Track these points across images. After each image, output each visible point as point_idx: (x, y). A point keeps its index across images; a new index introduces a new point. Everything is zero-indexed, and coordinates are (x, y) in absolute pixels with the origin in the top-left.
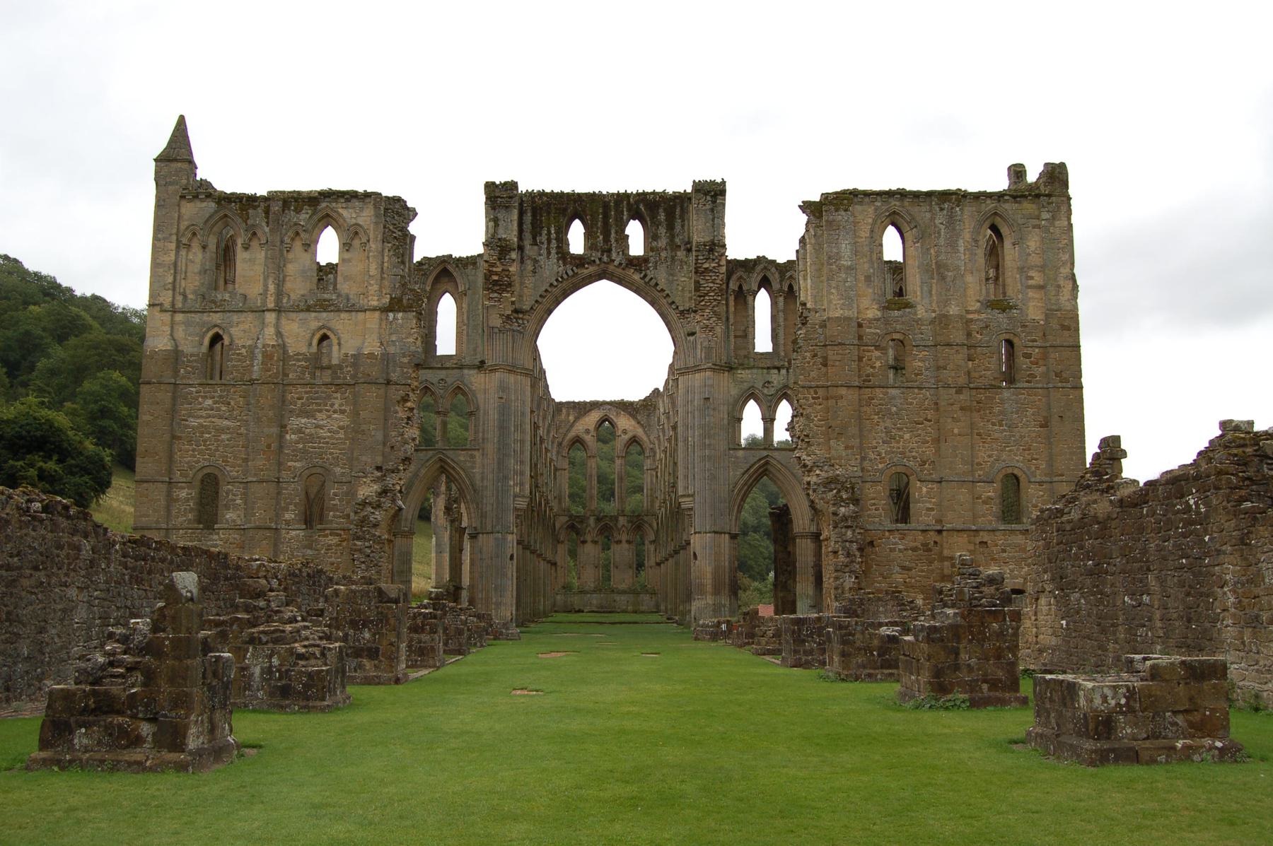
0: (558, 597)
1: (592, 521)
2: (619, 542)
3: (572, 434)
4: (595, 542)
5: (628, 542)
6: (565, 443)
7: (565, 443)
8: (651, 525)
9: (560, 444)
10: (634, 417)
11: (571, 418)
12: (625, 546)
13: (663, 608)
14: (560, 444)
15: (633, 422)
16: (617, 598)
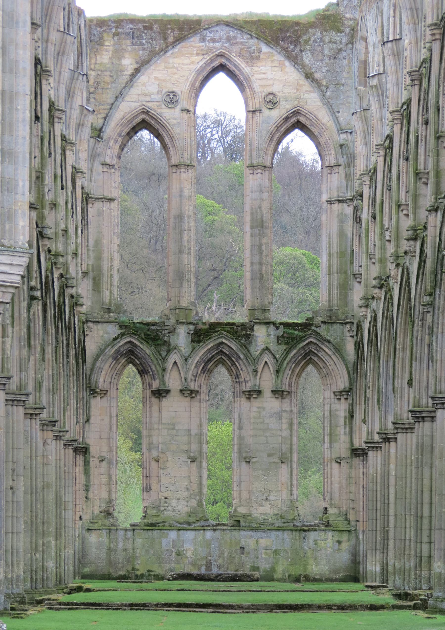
0: (93, 538)
1: (182, 338)
2: (254, 393)
3: (128, 107)
4: (189, 393)
5: (277, 393)
6: (112, 130)
7: (112, 130)
8: (339, 350)
9: (98, 133)
10: (295, 60)
11: (128, 63)
12: (270, 403)
13: (373, 566)
14: (98, 133)
15: (292, 74)
16: (247, 538)
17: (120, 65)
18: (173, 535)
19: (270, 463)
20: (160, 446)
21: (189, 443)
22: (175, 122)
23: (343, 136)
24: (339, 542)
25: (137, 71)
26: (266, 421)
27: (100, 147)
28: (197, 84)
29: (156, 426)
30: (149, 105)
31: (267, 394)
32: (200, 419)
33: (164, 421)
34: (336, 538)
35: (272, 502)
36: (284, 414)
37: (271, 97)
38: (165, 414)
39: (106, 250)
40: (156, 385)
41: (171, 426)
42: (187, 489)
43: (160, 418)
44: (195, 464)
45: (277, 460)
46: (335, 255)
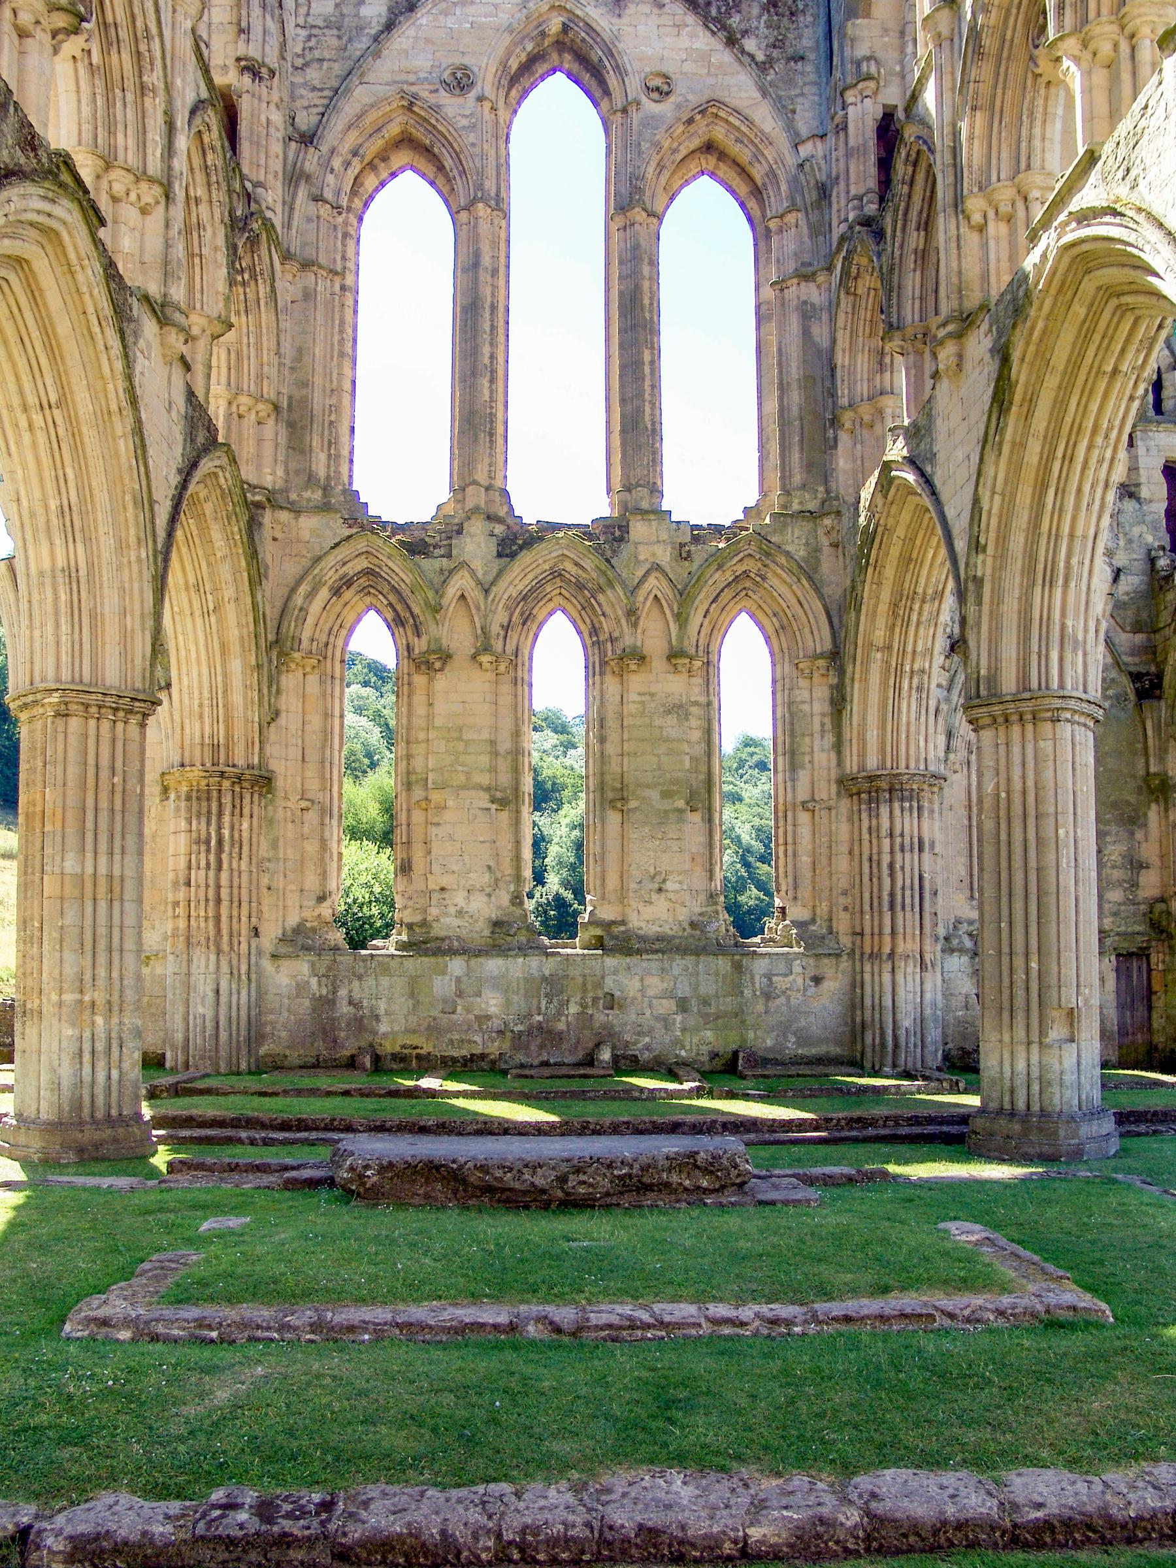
1: (477, 546)
7: (339, 135)
17: (357, 15)
18: (457, 966)
19: (666, 812)
20: (431, 776)
21: (493, 770)
22: (465, 122)
23: (805, 150)
24: (817, 980)
25: (389, 26)
26: (656, 723)
27: (311, 161)
28: (514, 65)
29: (422, 736)
30: (414, 89)
31: (658, 664)
32: (517, 719)
33: (438, 722)
34: (811, 972)
35: (671, 895)
36: (694, 710)
37: (658, 82)
38: (440, 707)
39: (319, 369)
40: (420, 645)
41: (455, 735)
42: (489, 867)
43: (430, 717)
44: (505, 816)
45: (681, 804)
46: (795, 385)
